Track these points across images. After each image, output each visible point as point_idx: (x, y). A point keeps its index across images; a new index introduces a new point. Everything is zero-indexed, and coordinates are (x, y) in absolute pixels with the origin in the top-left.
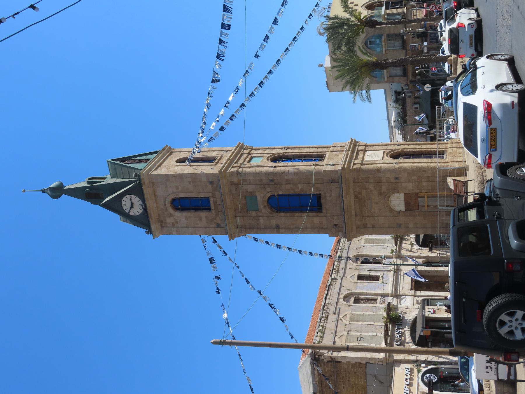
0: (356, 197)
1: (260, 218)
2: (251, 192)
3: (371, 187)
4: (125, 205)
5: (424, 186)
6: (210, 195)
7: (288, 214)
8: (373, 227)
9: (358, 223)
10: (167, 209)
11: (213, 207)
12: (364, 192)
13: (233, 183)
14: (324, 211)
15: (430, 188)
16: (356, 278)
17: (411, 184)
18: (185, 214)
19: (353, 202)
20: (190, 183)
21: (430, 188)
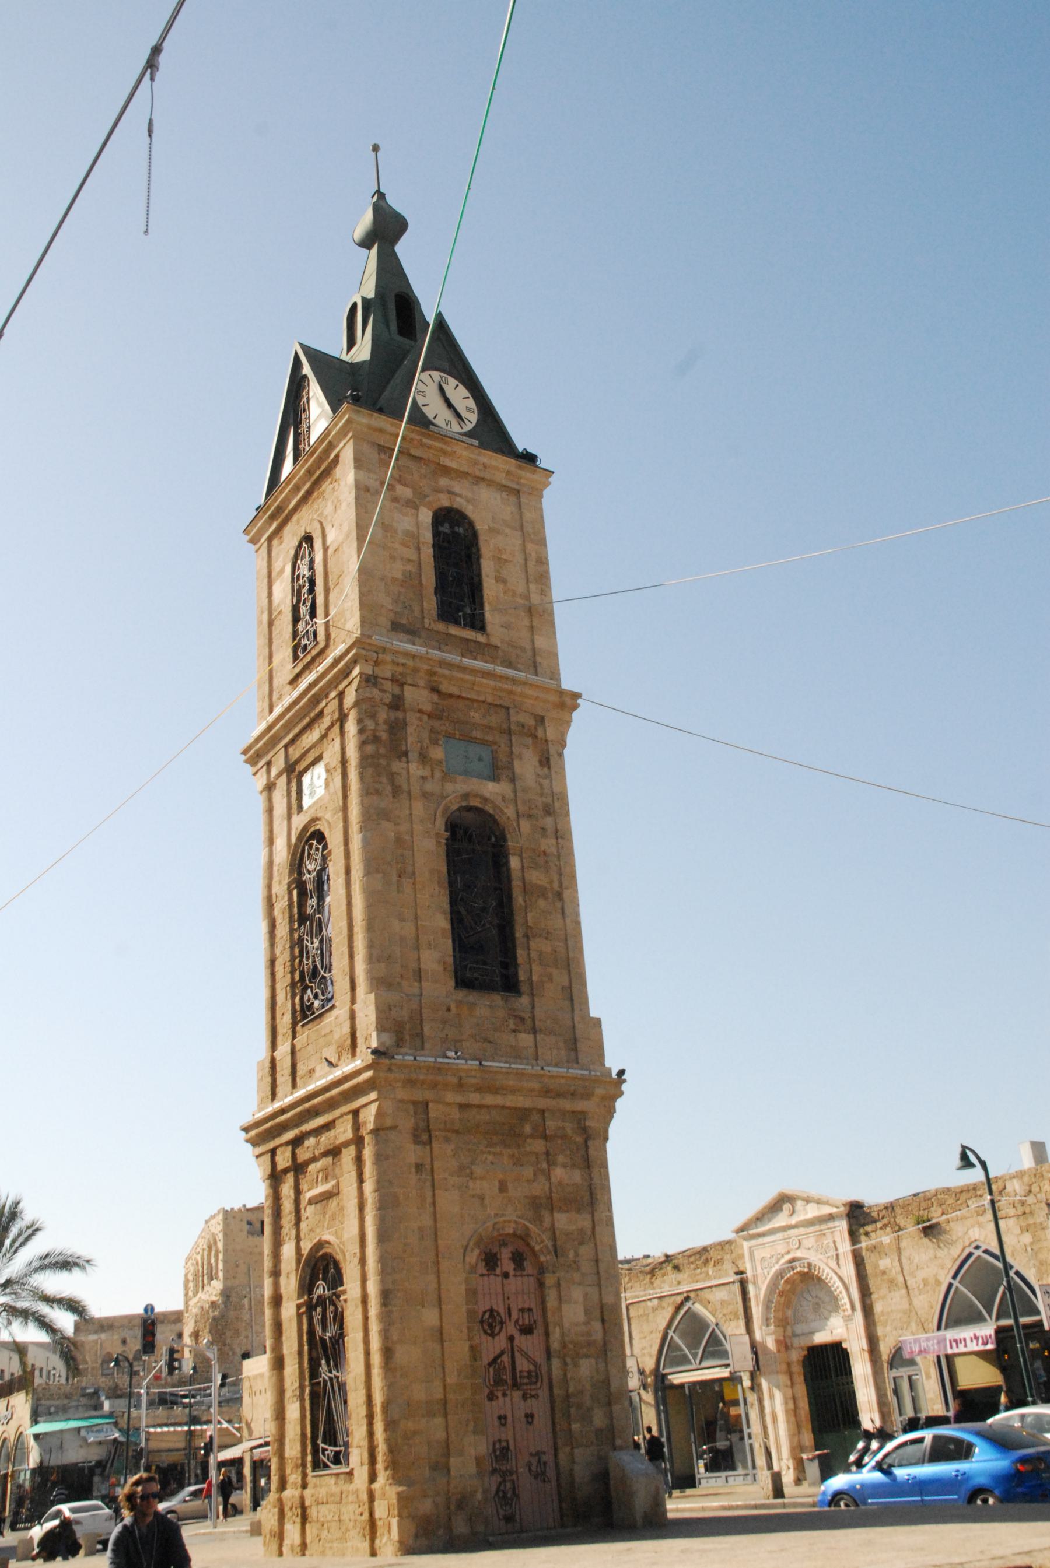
0: (523, 1114)
2: (510, 766)
3: (558, 1173)
5: (576, 1365)
6: (495, 641)
7: (445, 869)
8: (419, 1167)
9: (434, 1111)
10: (439, 491)
11: (454, 630)
12: (538, 1146)
13: (528, 724)
14: (461, 994)
17: (581, 1317)
18: (428, 536)
19: (511, 1101)
20: (527, 598)
21: (571, 1390)
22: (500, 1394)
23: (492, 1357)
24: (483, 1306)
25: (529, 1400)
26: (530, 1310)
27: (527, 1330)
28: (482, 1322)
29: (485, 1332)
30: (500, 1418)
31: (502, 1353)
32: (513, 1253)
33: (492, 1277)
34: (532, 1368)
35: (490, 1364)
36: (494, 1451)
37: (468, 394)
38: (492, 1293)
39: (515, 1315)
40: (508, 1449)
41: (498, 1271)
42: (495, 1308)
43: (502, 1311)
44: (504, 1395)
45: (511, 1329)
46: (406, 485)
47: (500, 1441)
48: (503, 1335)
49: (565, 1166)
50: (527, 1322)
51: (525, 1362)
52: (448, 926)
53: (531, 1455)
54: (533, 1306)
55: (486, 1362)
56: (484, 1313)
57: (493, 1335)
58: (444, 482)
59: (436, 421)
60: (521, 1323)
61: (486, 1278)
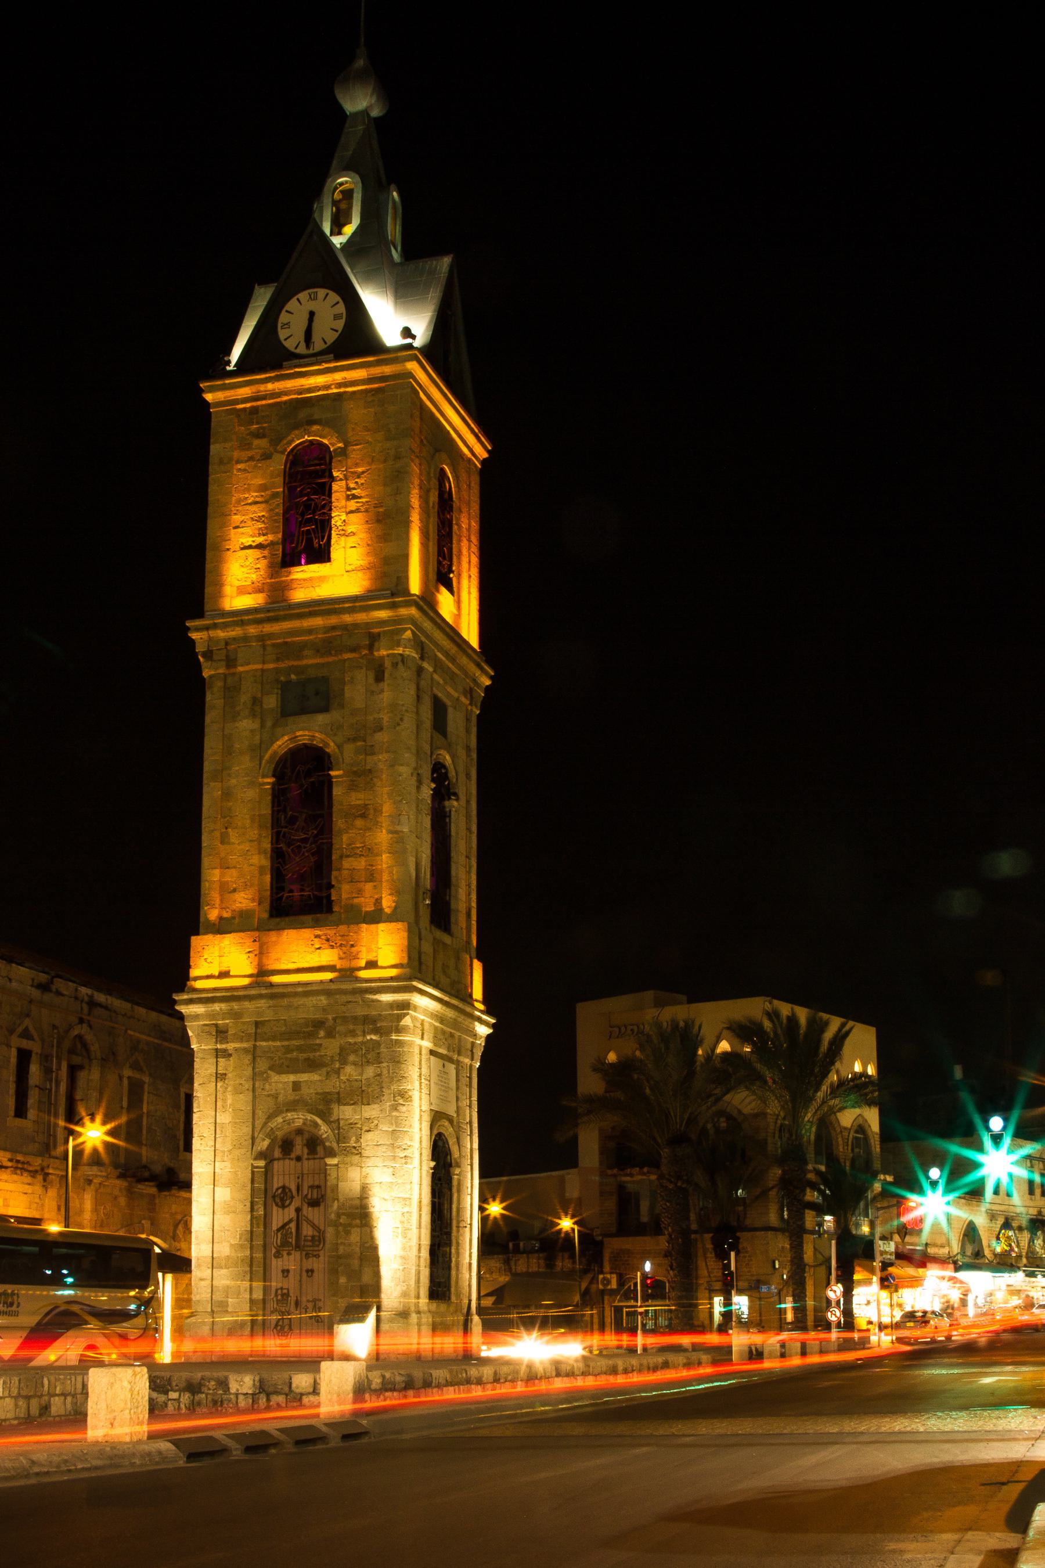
1: (258, 721)
3: (349, 1069)
4: (313, 298)
5: (348, 1233)
7: (266, 810)
10: (296, 426)
15: (341, 1250)
16: (25, 1044)
21: (341, 1250)
22: (285, 1253)
23: (280, 1224)
24: (277, 1183)
25: (310, 1259)
26: (318, 1187)
27: (314, 1203)
28: (274, 1197)
29: (277, 1205)
30: (283, 1271)
31: (290, 1221)
32: (308, 1141)
33: (287, 1161)
34: (316, 1233)
35: (278, 1230)
36: (276, 1295)
37: (338, 299)
38: (285, 1173)
39: (305, 1192)
40: (288, 1295)
41: (293, 1155)
42: (287, 1185)
43: (293, 1188)
44: (289, 1254)
45: (296, 1202)
46: (264, 436)
47: (282, 1289)
48: (292, 1208)
49: (355, 1064)
50: (315, 1196)
51: (310, 1229)
52: (266, 863)
53: (308, 1301)
54: (322, 1184)
55: (275, 1228)
56: (277, 1189)
57: (283, 1207)
58: (302, 414)
59: (298, 351)
60: (309, 1196)
61: (281, 1162)
